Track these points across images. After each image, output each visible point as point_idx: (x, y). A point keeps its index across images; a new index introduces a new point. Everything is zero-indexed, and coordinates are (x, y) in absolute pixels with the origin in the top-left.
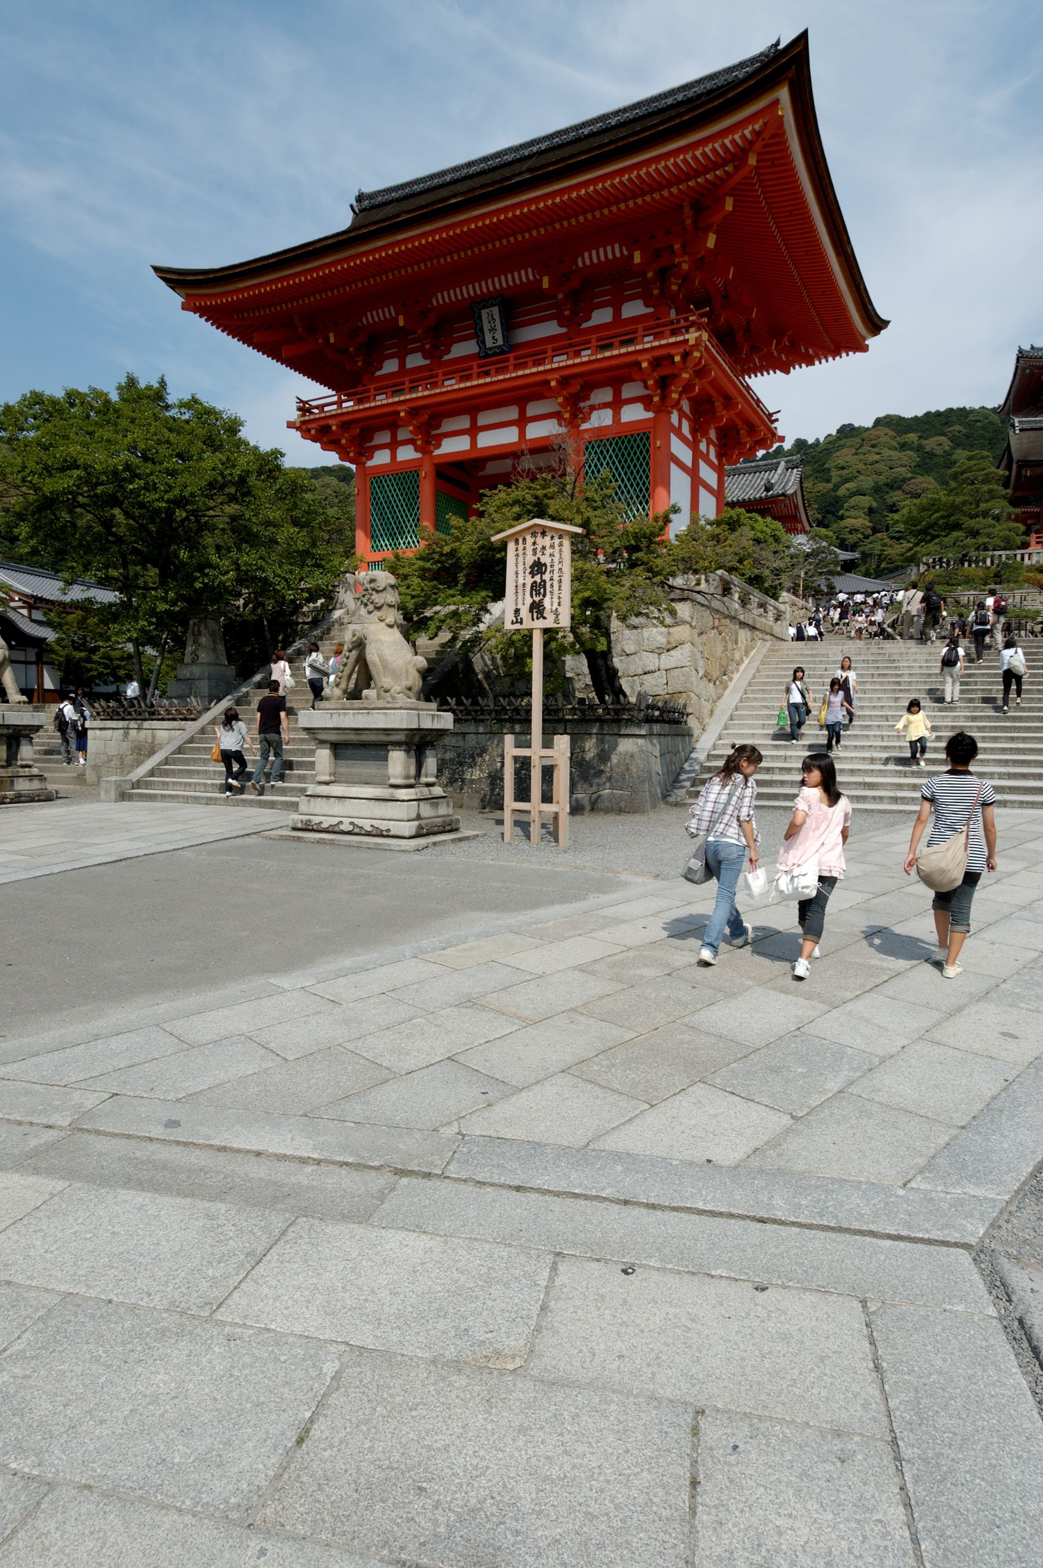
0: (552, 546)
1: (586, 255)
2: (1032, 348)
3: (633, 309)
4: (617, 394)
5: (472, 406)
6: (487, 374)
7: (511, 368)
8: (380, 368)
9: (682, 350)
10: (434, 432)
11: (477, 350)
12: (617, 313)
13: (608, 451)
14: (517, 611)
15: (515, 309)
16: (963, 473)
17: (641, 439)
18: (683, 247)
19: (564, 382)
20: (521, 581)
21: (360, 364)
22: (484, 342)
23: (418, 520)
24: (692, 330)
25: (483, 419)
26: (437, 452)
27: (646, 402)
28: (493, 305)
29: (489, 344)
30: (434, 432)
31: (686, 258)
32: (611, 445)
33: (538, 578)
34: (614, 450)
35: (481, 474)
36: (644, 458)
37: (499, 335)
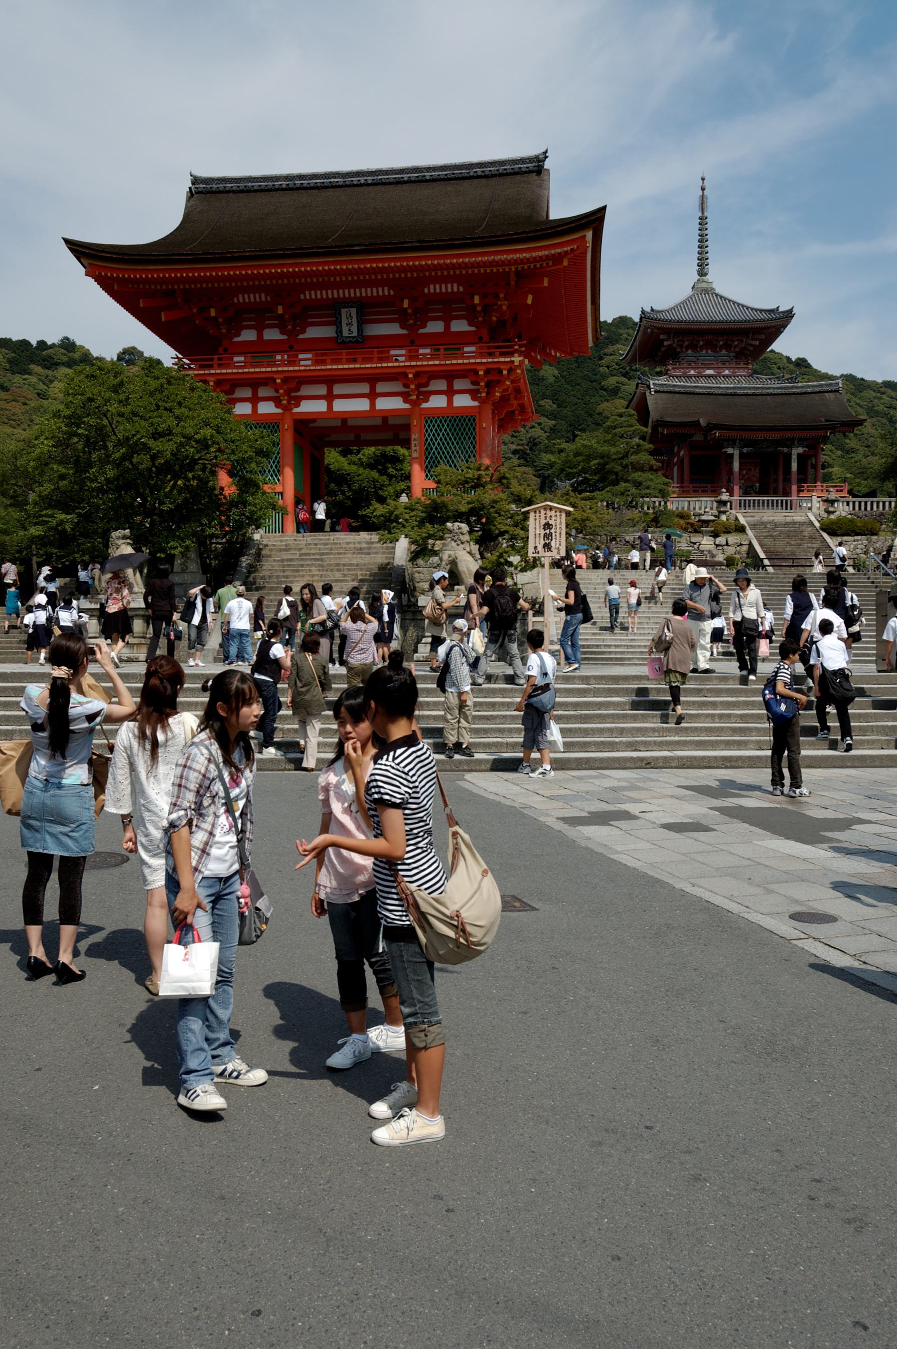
0: (556, 516)
1: (432, 286)
2: (652, 310)
3: (459, 326)
4: (450, 385)
5: (330, 381)
6: (355, 361)
7: (375, 359)
8: (239, 335)
9: (508, 367)
10: (293, 394)
11: (334, 335)
12: (447, 327)
13: (443, 426)
14: (536, 547)
15: (367, 311)
16: (615, 428)
17: (469, 420)
18: (505, 295)
19: (417, 375)
20: (538, 532)
21: (224, 331)
22: (341, 331)
23: (278, 462)
24: (516, 355)
25: (338, 389)
26: (296, 410)
27: (474, 394)
28: (352, 307)
29: (345, 333)
30: (293, 394)
31: (506, 302)
32: (446, 421)
33: (547, 531)
34: (448, 425)
35: (311, 425)
36: (472, 434)
37: (354, 329)
